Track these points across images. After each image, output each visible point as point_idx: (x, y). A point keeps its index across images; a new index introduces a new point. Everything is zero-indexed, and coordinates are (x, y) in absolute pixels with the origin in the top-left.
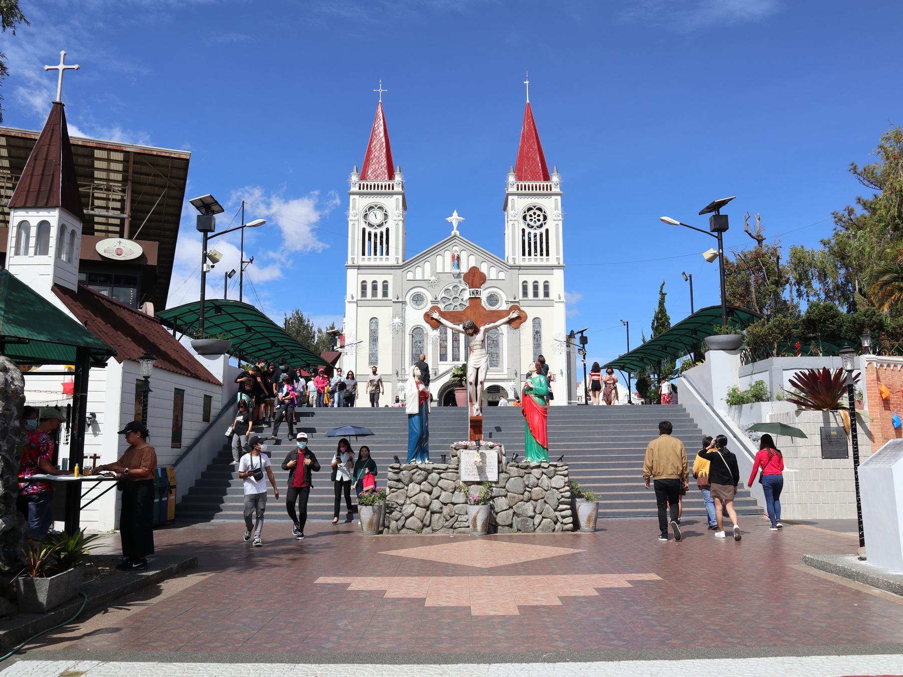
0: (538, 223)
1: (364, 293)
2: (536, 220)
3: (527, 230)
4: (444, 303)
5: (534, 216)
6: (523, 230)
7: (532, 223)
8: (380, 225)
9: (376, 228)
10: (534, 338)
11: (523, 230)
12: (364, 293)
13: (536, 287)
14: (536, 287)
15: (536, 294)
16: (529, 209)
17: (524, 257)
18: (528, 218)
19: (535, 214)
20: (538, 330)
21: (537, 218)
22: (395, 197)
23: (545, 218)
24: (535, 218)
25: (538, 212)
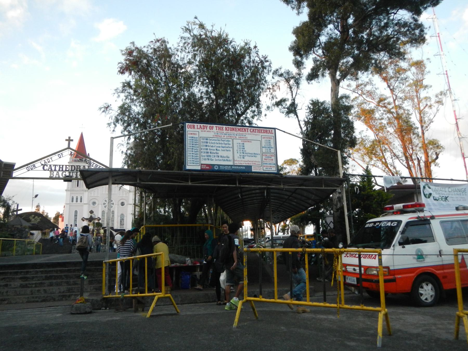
1: (72, 201)
12: (72, 201)
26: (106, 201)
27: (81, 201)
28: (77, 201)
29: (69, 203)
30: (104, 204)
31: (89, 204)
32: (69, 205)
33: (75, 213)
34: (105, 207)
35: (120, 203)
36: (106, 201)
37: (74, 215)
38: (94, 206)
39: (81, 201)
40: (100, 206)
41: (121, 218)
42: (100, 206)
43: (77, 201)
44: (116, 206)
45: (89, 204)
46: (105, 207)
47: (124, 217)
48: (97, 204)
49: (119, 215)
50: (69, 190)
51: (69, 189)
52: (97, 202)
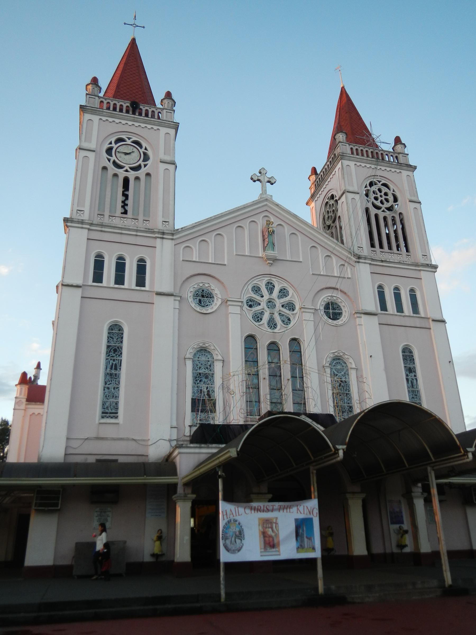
0: (387, 205)
1: (98, 277)
2: (383, 199)
3: (373, 211)
4: (251, 306)
5: (379, 194)
6: (367, 210)
7: (378, 203)
8: (137, 168)
9: (127, 171)
10: (407, 380)
11: (367, 210)
12: (98, 277)
13: (398, 297)
14: (398, 297)
15: (400, 308)
16: (371, 184)
17: (373, 249)
18: (372, 196)
19: (380, 190)
20: (411, 366)
21: (384, 197)
22: (163, 130)
23: (396, 200)
24: (381, 196)
25: (384, 189)
26: (256, 290)
27: (141, 282)
28: (120, 279)
29: (79, 282)
30: (251, 303)
31: (181, 299)
32: (78, 292)
33: (110, 337)
34: (258, 318)
35: (320, 304)
36: (256, 290)
37: (104, 349)
38: (204, 311)
39: (141, 282)
40: (234, 310)
41: (333, 375)
42: (234, 310)
43: (120, 279)
44: (308, 316)
45: (181, 299)
46: (258, 318)
47: (346, 374)
48: (217, 303)
49: (326, 361)
50: (82, 222)
51: (86, 217)
52: (217, 291)
